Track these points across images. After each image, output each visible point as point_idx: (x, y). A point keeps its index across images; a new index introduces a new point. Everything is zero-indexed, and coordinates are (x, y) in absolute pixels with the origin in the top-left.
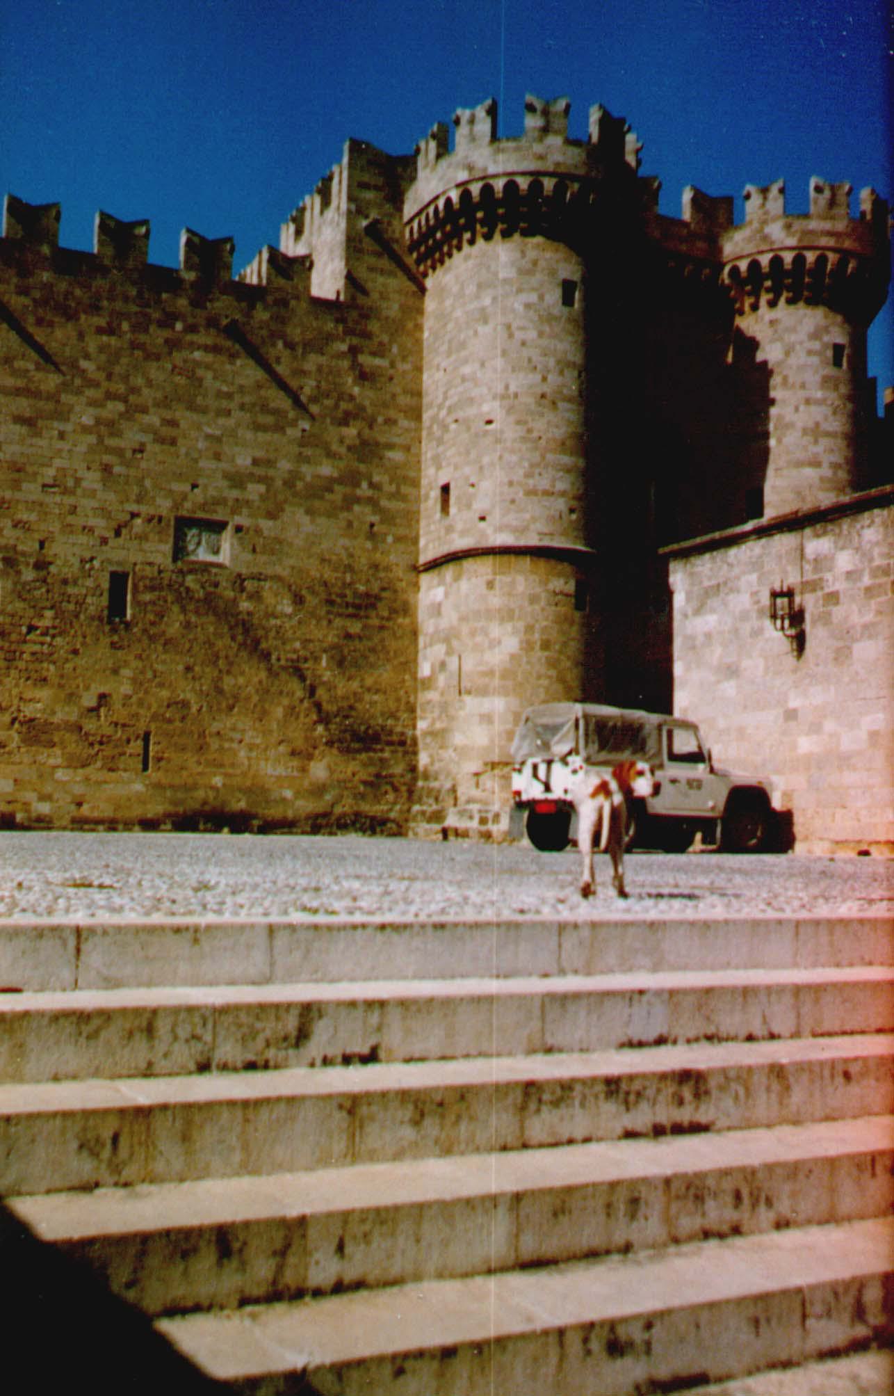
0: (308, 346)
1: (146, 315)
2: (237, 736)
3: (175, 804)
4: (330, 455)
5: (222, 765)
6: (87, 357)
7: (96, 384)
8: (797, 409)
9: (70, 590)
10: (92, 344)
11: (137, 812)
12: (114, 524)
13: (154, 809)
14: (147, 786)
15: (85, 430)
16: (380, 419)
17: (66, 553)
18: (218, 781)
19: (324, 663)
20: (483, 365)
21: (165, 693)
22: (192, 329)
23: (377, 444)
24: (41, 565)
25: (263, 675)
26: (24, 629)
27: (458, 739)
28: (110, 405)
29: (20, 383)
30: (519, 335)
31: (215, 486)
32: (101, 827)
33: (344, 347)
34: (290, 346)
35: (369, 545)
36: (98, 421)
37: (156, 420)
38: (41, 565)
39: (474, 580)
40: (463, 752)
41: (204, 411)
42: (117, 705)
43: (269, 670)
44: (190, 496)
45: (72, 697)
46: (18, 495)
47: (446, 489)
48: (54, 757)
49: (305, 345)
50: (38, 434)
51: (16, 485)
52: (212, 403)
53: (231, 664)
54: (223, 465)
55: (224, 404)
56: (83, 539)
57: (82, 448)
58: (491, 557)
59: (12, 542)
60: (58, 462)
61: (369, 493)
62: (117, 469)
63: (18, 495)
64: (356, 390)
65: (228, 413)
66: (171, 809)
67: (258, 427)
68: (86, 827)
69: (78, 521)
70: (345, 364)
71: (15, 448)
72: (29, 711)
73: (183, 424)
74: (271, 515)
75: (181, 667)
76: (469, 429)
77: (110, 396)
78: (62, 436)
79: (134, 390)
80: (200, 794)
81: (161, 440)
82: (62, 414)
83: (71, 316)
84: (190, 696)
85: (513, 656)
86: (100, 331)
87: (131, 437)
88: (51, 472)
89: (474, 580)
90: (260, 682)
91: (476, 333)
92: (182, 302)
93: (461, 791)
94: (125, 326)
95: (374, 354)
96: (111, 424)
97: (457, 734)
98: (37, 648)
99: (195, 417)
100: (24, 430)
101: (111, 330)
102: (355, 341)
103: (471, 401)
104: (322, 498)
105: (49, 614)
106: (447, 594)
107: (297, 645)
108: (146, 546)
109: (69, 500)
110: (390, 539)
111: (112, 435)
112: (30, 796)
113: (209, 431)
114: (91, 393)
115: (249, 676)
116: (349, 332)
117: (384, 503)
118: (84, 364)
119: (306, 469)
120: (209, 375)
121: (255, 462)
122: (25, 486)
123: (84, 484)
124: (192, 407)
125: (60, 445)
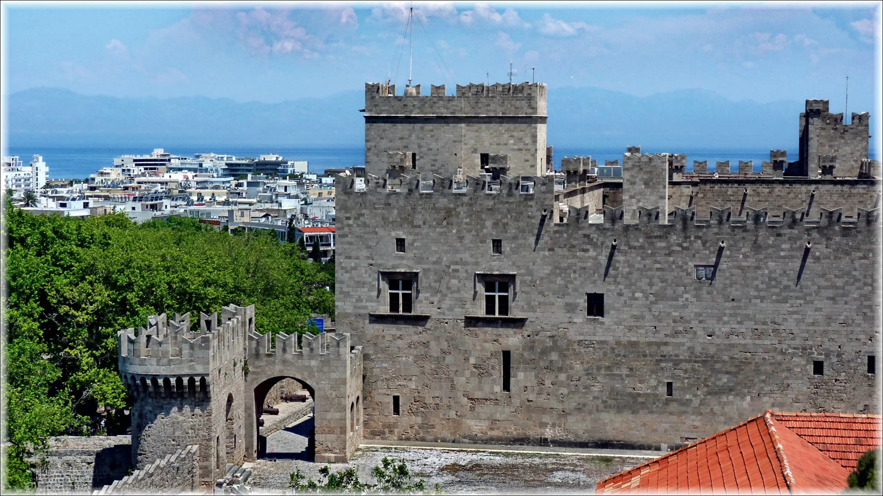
6: (855, 270)
7: (859, 280)
9: (852, 365)
15: (855, 299)
17: (849, 349)
24: (839, 355)
28: (865, 288)
29: (829, 284)
36: (861, 295)
38: (839, 355)
46: (829, 328)
50: (837, 304)
56: (854, 344)
60: (845, 314)
63: (829, 328)
77: (865, 284)
78: (846, 303)
86: (861, 258)
88: (842, 317)
96: (865, 296)
109: (850, 329)
114: (857, 284)
118: (854, 273)
122: (833, 324)
125: (846, 306)
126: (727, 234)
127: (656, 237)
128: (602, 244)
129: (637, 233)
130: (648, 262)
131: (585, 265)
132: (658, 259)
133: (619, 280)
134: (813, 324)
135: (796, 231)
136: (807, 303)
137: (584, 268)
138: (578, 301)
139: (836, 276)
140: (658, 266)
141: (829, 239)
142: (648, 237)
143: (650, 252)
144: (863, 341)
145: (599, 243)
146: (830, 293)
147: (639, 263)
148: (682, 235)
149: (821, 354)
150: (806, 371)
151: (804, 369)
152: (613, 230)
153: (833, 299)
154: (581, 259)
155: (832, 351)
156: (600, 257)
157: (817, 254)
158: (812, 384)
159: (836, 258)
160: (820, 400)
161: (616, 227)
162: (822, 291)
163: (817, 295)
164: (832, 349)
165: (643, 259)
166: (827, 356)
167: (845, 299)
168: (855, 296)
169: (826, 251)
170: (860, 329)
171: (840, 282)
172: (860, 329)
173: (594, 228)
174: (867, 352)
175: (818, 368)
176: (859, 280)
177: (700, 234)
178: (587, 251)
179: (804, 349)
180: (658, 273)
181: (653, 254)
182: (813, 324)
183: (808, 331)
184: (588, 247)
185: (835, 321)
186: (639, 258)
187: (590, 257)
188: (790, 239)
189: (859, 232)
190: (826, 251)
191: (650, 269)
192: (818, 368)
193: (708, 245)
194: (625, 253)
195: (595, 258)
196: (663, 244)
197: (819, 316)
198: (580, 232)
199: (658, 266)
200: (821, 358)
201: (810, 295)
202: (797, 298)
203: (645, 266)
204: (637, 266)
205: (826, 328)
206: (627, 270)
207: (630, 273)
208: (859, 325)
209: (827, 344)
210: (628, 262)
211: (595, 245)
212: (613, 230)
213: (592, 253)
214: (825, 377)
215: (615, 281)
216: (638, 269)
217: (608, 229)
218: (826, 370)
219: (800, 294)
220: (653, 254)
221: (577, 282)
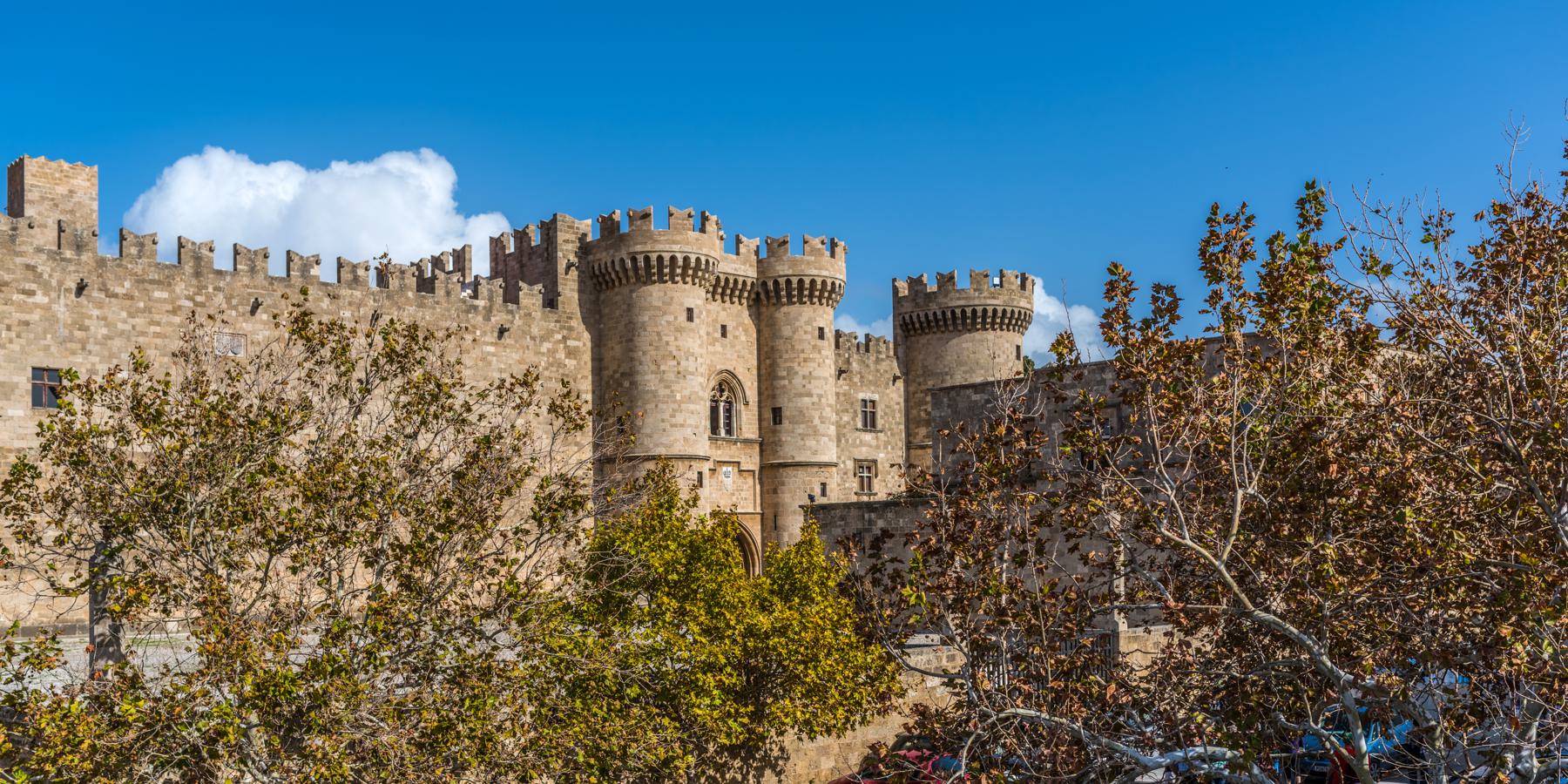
0: (544, 339)
22: (484, 333)
30: (665, 339)
33: (559, 337)
34: (533, 339)
92: (480, 318)
102: (565, 332)
116: (562, 328)
126: (263, 288)
127: (152, 282)
128: (60, 283)
129: (120, 271)
130: (140, 321)
131: (27, 317)
132: (157, 317)
133: (89, 347)
135: (357, 294)
137: (27, 323)
138: (15, 379)
140: (158, 329)
142: (140, 281)
143: (142, 305)
145: (54, 283)
147: (125, 322)
148: (194, 282)
152: (79, 263)
154: (21, 307)
156: (55, 307)
161: (84, 257)
165: (131, 315)
173: (44, 257)
177: (222, 284)
178: (31, 293)
180: (158, 341)
181: (148, 310)
184: (34, 286)
186: (124, 314)
187: (37, 305)
188: (350, 304)
191: (143, 334)
193: (234, 302)
194: (100, 305)
195: (47, 308)
196: (165, 295)
198: (18, 260)
199: (158, 329)
203: (134, 327)
204: (120, 326)
206: (104, 331)
207: (107, 338)
210: (105, 319)
211: (46, 288)
212: (79, 263)
213: (40, 298)
215: (83, 349)
216: (122, 332)
217: (69, 261)
220: (148, 310)
221: (16, 347)
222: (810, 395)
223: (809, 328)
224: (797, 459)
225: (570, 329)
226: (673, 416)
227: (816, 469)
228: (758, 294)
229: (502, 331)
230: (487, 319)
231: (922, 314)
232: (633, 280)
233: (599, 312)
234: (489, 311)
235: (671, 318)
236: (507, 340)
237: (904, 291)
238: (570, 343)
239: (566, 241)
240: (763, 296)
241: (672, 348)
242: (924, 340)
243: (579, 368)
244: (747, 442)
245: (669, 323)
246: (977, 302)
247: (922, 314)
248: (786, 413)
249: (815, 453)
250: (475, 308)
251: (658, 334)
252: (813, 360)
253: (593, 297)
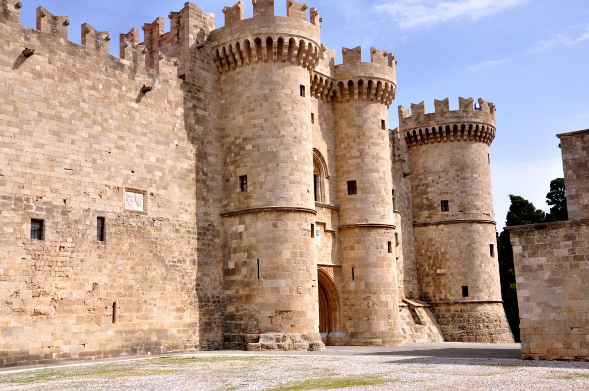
1: (110, 81)
2: (152, 302)
3: (126, 341)
4: (188, 158)
5: (147, 318)
6: (84, 101)
7: (88, 116)
8: (369, 147)
9: (80, 227)
10: (86, 93)
11: (109, 348)
12: (98, 191)
13: (117, 344)
14: (114, 332)
16: (206, 141)
17: (77, 205)
18: (146, 327)
19: (187, 263)
20: (266, 120)
21: (122, 281)
22: (129, 90)
23: (205, 153)
25: (164, 270)
26: (58, 249)
27: (259, 300)
29: (53, 113)
30: (284, 108)
31: (141, 171)
32: (93, 357)
34: (170, 102)
35: (203, 202)
36: (91, 136)
37: (116, 137)
38: (64, 213)
39: (265, 223)
40: (263, 306)
41: (135, 133)
42: (101, 290)
43: (166, 266)
44: (131, 177)
45: (81, 286)
46: (52, 174)
47: (243, 178)
48: (71, 320)
49: (176, 103)
51: (52, 168)
52: (138, 129)
53: (150, 265)
54: (145, 162)
55: (145, 130)
56: (83, 198)
57: (83, 149)
58: (275, 213)
59: (50, 200)
60: (71, 157)
61: (203, 177)
62: (99, 161)
63: (52, 174)
64: (196, 127)
65: (145, 135)
66: (125, 344)
67: (158, 143)
68: (86, 357)
69: (82, 190)
70: (192, 113)
71: (52, 148)
72: (60, 294)
73: (127, 139)
74: (165, 188)
75: (128, 268)
76: (259, 150)
77: (95, 122)
78: (73, 142)
79: (106, 120)
80: (137, 335)
81: (118, 147)
82: (73, 132)
83: (75, 78)
84: (133, 283)
85: (287, 260)
87: (106, 144)
88: (68, 161)
89: (265, 223)
90: (163, 274)
91: (261, 105)
92: (125, 76)
93: (261, 325)
94: (101, 87)
95: (202, 109)
97: (257, 297)
98: (63, 259)
99: (133, 136)
100: (55, 138)
101: (94, 88)
102: (195, 102)
103: (260, 137)
104: (184, 179)
105: (69, 239)
106: (246, 229)
107: (176, 254)
108: (114, 203)
109: (77, 178)
110: (211, 201)
111: (96, 143)
112: (60, 342)
113: (138, 143)
114: (86, 120)
115: (157, 271)
117: (208, 183)
118: (83, 105)
119: (178, 165)
120: (138, 114)
121: (158, 160)
122: (56, 169)
123: (84, 169)
124: (129, 131)
125: (73, 147)
134: (31, 165)
136: (23, 133)
139: (61, 104)
141: (52, 52)
144: (92, 195)
146: (54, 125)
149: (41, 209)
150: (21, 231)
151: (18, 230)
153: (57, 134)
155: (55, 207)
157: (38, 68)
158: (28, 252)
159: (61, 80)
160: (39, 278)
162: (44, 120)
163: (36, 125)
164: (55, 203)
166: (50, 211)
167: (72, 137)
168: (84, 135)
169: (50, 68)
170: (88, 180)
171: (66, 114)
172: (88, 180)
174: (96, 211)
175: (38, 228)
176: (88, 116)
179: (18, 199)
182: (31, 165)
183: (24, 175)
185: (60, 164)
189: (88, 54)
190: (50, 68)
192: (38, 228)
197: (40, 156)
200: (42, 215)
201: (28, 122)
202: (9, 124)
205: (48, 173)
208: (87, 175)
209: (49, 197)
214: (47, 243)
218: (48, 232)
219: (13, 119)
222: (378, 171)
223: (375, 120)
224: (371, 222)
225: (199, 99)
226: (291, 174)
227: (384, 230)
228: (335, 92)
229: (145, 90)
230: (132, 77)
231: (423, 130)
232: (255, 59)
233: (221, 90)
234: (134, 70)
235: (289, 92)
236: (148, 98)
237: (408, 113)
238: (198, 111)
239: (196, 27)
240: (339, 94)
241: (289, 116)
242: (424, 148)
243: (205, 133)
244: (328, 207)
245: (286, 95)
246: (465, 120)
247: (423, 130)
248: (358, 185)
249: (383, 217)
250: (122, 66)
251: (278, 104)
252: (379, 144)
253: (216, 77)
